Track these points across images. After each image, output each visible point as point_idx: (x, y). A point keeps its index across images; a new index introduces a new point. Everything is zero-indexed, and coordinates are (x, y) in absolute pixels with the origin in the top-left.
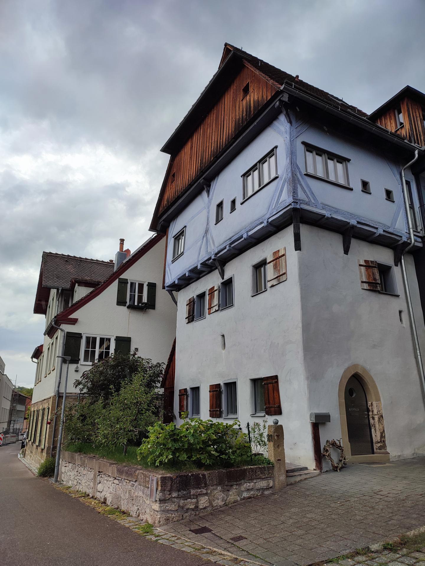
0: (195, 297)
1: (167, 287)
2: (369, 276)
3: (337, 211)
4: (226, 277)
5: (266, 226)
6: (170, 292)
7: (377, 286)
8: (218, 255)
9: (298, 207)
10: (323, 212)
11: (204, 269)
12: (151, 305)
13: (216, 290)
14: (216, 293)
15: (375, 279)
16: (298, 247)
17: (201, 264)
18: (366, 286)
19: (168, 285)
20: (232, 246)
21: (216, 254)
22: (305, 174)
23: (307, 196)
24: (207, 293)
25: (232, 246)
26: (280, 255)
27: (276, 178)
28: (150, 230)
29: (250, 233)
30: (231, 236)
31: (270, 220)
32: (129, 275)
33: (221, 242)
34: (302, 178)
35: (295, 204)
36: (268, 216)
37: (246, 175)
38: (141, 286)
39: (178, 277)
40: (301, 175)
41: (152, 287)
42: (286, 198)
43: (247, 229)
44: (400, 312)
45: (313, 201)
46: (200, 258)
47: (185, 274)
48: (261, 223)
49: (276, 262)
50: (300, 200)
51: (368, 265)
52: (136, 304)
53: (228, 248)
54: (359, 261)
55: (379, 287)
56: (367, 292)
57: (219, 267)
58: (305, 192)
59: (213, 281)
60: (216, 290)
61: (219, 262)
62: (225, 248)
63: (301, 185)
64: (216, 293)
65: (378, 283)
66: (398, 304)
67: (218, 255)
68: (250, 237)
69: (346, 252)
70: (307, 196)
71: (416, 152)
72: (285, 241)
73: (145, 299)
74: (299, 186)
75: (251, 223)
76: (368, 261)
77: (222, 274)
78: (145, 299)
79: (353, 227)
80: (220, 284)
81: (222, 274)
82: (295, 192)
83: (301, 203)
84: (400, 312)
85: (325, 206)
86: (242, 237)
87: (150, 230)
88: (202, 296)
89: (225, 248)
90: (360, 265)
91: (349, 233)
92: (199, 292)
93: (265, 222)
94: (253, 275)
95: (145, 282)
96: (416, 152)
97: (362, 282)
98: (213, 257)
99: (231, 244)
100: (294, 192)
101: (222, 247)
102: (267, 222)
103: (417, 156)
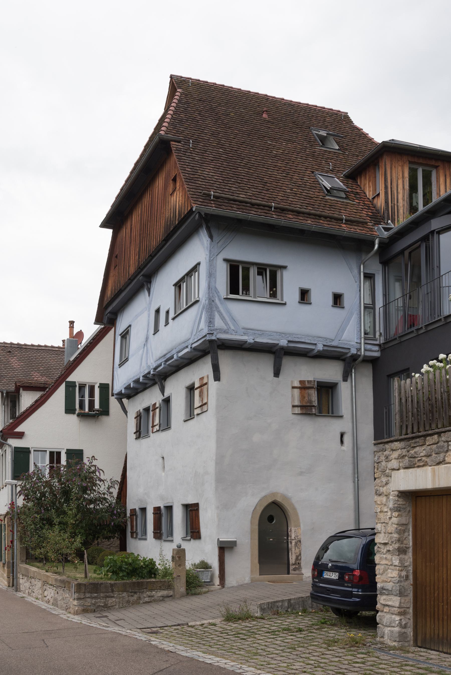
0: (141, 410)
1: (116, 394)
2: (302, 397)
3: (262, 333)
4: (166, 394)
5: (190, 352)
6: (120, 400)
7: (312, 409)
8: (157, 370)
9: (213, 338)
10: (245, 338)
11: (146, 381)
12: (105, 411)
13: (157, 408)
14: (158, 410)
15: (311, 401)
16: (217, 378)
17: (143, 376)
18: (298, 410)
19: (116, 393)
20: (167, 363)
21: (155, 369)
22: (224, 298)
23: (226, 324)
24: (151, 409)
25: (167, 363)
26: (204, 383)
27: (197, 302)
28: (95, 324)
29: (180, 354)
30: (165, 352)
31: (194, 346)
32: (77, 377)
33: (158, 358)
34: (221, 303)
35: (211, 335)
36: (191, 341)
37: (178, 285)
38: (92, 388)
39: (125, 386)
40: (220, 300)
41: (104, 388)
42: (204, 327)
43: (177, 350)
44: (342, 435)
45: (232, 328)
46: (142, 370)
47: (130, 385)
48: (187, 347)
49: (201, 390)
50: (216, 329)
51: (304, 387)
52: (87, 410)
53: (163, 366)
54: (292, 382)
55: (314, 410)
56: (299, 417)
57: (159, 383)
58: (223, 318)
59: (153, 397)
60: (157, 408)
61: (158, 378)
62: (160, 365)
63: (219, 312)
64: (158, 410)
65: (314, 406)
66: (344, 425)
67: (157, 370)
68: (181, 358)
69: (277, 374)
70: (226, 324)
71: (377, 241)
72: (204, 369)
73: (97, 406)
74: (216, 313)
75: (180, 344)
76: (304, 381)
77: (162, 391)
78: (97, 406)
79: (282, 348)
80: (161, 401)
81: (162, 391)
82: (210, 322)
83: (217, 333)
84: (342, 435)
85: (247, 330)
86: (172, 357)
87: (95, 324)
88: (147, 410)
89: (160, 365)
90: (293, 388)
91: (279, 354)
92: (145, 405)
93: (189, 347)
94: (186, 397)
95: (96, 383)
96: (377, 241)
97: (294, 406)
98: (152, 373)
99: (166, 361)
100: (210, 322)
101: (159, 362)
102: (191, 348)
103: (376, 247)
